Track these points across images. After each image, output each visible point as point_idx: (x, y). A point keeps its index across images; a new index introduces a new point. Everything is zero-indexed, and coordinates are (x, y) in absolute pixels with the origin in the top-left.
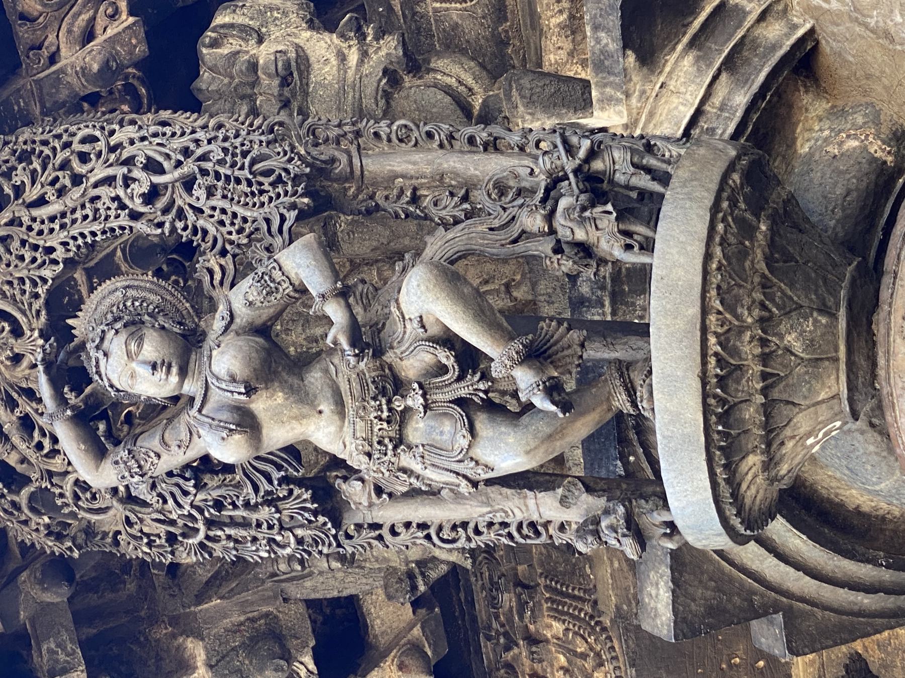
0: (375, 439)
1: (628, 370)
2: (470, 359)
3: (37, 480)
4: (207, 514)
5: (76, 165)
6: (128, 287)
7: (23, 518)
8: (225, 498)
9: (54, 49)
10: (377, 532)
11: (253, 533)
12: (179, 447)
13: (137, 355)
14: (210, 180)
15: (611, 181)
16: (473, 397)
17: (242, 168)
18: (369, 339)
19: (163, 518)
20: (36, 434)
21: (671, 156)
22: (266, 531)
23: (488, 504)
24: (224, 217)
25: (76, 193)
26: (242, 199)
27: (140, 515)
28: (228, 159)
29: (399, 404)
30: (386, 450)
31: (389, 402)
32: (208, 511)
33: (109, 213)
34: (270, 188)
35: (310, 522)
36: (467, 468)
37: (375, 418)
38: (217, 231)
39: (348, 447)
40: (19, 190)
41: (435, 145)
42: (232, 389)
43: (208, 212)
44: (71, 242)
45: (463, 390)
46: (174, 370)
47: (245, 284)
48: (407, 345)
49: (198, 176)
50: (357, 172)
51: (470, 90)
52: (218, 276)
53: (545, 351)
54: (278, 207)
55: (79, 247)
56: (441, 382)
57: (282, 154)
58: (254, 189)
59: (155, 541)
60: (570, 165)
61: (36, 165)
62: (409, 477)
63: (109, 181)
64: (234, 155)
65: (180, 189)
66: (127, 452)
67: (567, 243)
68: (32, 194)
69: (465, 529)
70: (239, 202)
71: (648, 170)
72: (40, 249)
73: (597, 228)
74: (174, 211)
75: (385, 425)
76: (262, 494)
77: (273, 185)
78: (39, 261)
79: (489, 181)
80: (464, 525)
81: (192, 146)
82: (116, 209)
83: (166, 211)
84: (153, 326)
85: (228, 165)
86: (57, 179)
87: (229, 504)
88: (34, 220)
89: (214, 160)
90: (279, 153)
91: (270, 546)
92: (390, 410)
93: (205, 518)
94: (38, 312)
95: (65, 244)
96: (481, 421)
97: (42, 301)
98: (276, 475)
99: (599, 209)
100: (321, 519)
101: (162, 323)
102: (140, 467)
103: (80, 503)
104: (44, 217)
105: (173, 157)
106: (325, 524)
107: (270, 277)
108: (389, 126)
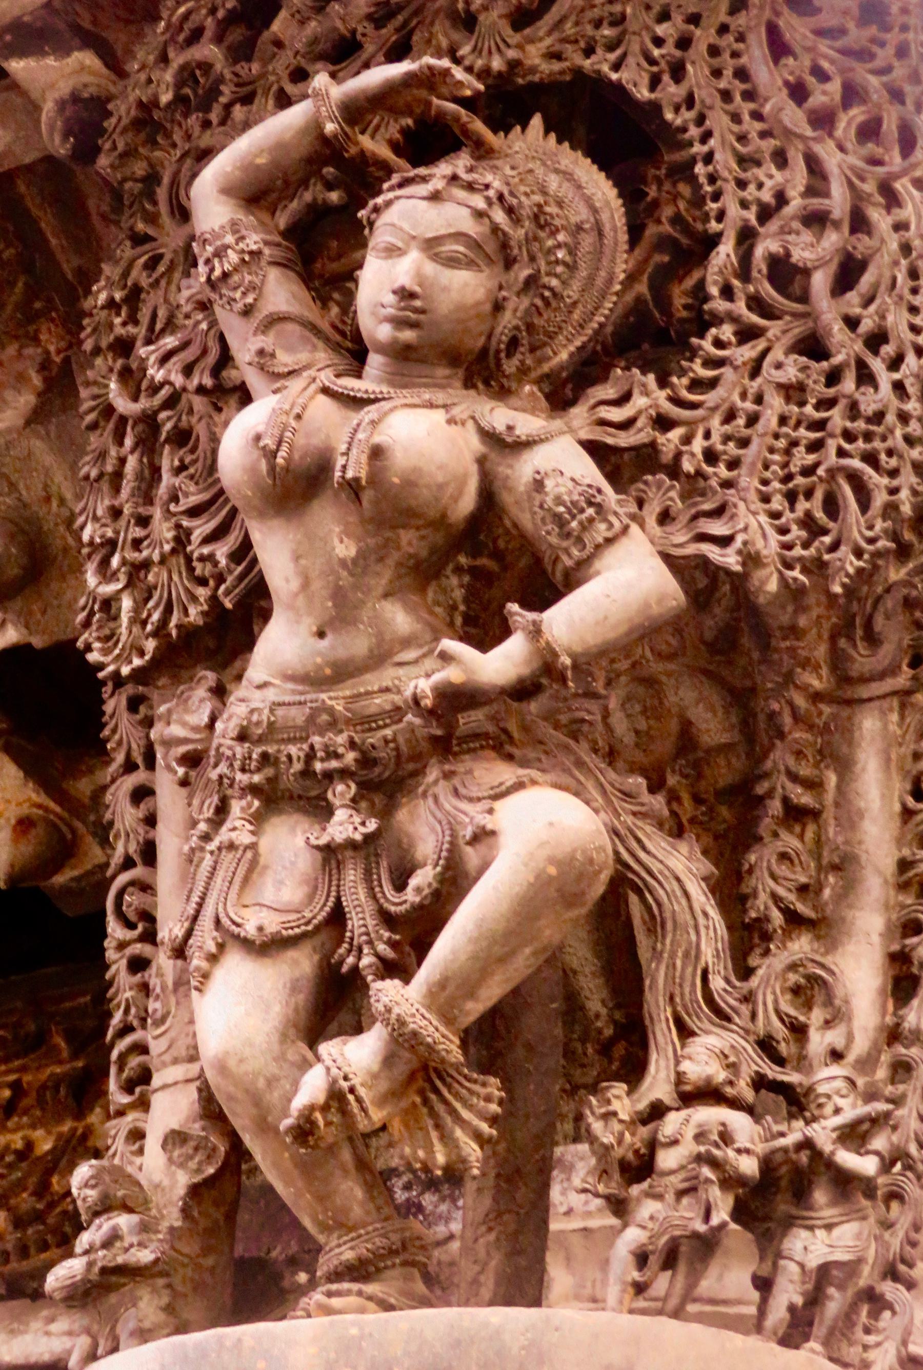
0: (271, 749)
1: (405, 1264)
2: (416, 932)
3: (236, 75)
4: (163, 415)
5: (858, 114)
6: (601, 234)
7: (171, 54)
8: (193, 451)
10: (139, 761)
12: (261, 353)
13: (436, 258)
15: (789, 1223)
16: (346, 945)
17: (841, 453)
18: (459, 727)
21: (866, 1347)
22: (130, 537)
24: (741, 421)
25: (794, 117)
26: (776, 457)
27: (163, 283)
28: (860, 425)
29: (341, 792)
30: (251, 772)
31: (344, 774)
32: (169, 418)
33: (752, 188)
35: (144, 623)
36: (206, 938)
37: (312, 747)
38: (714, 409)
39: (258, 694)
41: (906, 852)
43: (754, 386)
44: (690, 115)
46: (408, 335)
47: (587, 471)
48: (447, 806)
49: (825, 364)
50: (849, 693)
52: (616, 414)
53: (437, 1091)
54: (754, 532)
56: (379, 880)
57: (869, 534)
58: (799, 480)
59: (118, 314)
60: (823, 1133)
62: (209, 821)
64: (868, 437)
65: (799, 329)
66: (254, 247)
67: (656, 1132)
70: (772, 450)
71: (815, 1299)
72: (678, 53)
73: (681, 1194)
75: (297, 767)
76: (185, 523)
77: (808, 522)
78: (656, 52)
79: (823, 966)
81: (888, 350)
82: (759, 203)
83: (757, 303)
84: (501, 288)
85: (848, 424)
86: (823, 76)
87: (181, 460)
88: (741, 38)
89: (857, 396)
90: (871, 527)
91: (102, 545)
92: (329, 776)
93: (156, 413)
94: (556, 56)
95: (690, 102)
96: (302, 963)
98: (222, 551)
101: (510, 305)
102: (225, 275)
103: (189, 162)
104: (744, 60)
105: (865, 313)
106: (142, 653)
107: (591, 520)
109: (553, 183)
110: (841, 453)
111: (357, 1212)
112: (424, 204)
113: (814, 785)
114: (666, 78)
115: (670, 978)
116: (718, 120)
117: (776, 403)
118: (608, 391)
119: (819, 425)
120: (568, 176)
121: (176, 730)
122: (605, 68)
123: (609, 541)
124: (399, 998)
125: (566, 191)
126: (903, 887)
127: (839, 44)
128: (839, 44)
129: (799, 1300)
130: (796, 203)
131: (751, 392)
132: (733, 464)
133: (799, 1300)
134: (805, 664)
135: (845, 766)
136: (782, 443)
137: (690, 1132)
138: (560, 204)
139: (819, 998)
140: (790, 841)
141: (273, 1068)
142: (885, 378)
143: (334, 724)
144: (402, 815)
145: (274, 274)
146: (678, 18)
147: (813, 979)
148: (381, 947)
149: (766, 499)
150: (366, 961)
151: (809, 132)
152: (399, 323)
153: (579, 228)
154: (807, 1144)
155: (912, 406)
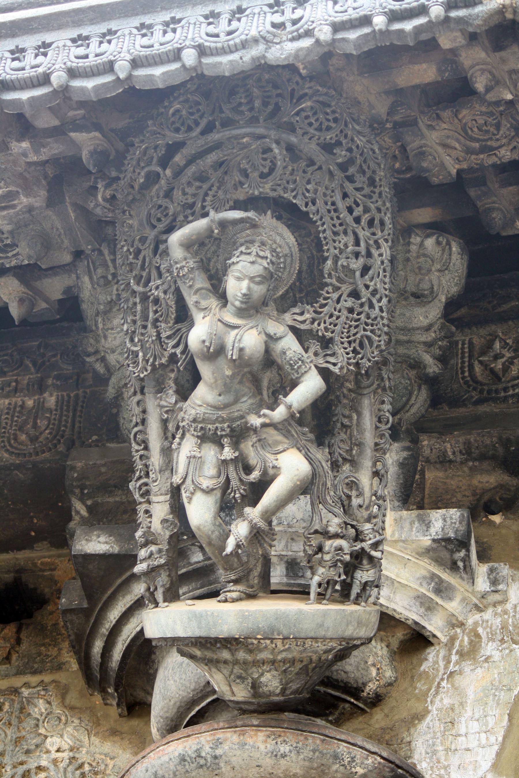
9: (437, 128)
11: (139, 323)
12: (196, 302)
13: (253, 282)
14: (358, 309)
19: (147, 264)
20: (198, 184)
23: (160, 471)
24: (334, 318)
25: (349, 219)
28: (369, 321)
31: (226, 436)
34: (352, 348)
38: (326, 314)
39: (198, 408)
40: (350, 179)
42: (235, 350)
43: (338, 306)
44: (318, 217)
45: (234, 483)
51: (407, 411)
52: (300, 318)
55: (316, 222)
60: (366, 545)
61: (367, 190)
63: (357, 243)
64: (372, 325)
65: (350, 288)
68: (349, 187)
69: (143, 449)
73: (330, 567)
74: (339, 285)
78: (307, 194)
80: (146, 448)
81: (378, 296)
83: (339, 280)
90: (373, 353)
94: (275, 190)
96: (218, 494)
97: (282, 194)
98: (178, 351)
99: (342, 570)
100: (149, 368)
106: (147, 371)
108: (388, 411)
109: (278, 239)
110: (365, 330)
111: (235, 565)
112: (249, 264)
113: (350, 417)
114: (310, 204)
115: (318, 491)
116: (327, 219)
117: (345, 312)
118: (297, 310)
119: (359, 320)
120: (281, 235)
121: (163, 403)
122: (291, 198)
123: (306, 372)
124: (254, 513)
125: (282, 243)
126: (376, 450)
127: (362, 193)
128: (362, 193)
129: (359, 591)
130: (350, 248)
131: (338, 308)
132: (332, 332)
133: (359, 591)
134: (347, 381)
135: (359, 415)
136: (347, 326)
137: (333, 550)
138: (280, 247)
139: (354, 488)
140: (343, 436)
141: (213, 528)
142: (377, 306)
143: (223, 421)
144: (242, 446)
145: (197, 273)
146: (313, 183)
147: (352, 481)
148: (242, 491)
149: (342, 343)
150: (237, 495)
151: (355, 225)
152: (242, 302)
153: (286, 255)
154: (363, 549)
155: (384, 314)
